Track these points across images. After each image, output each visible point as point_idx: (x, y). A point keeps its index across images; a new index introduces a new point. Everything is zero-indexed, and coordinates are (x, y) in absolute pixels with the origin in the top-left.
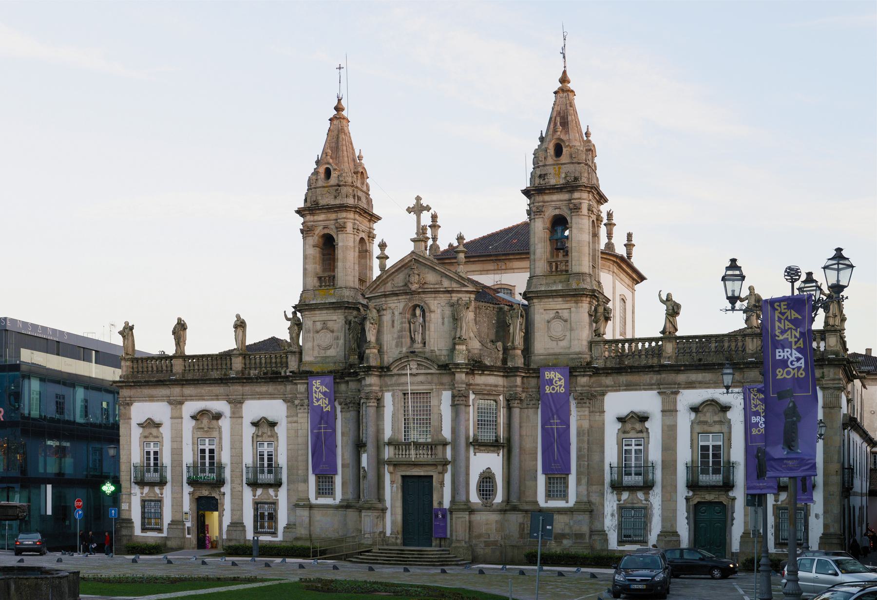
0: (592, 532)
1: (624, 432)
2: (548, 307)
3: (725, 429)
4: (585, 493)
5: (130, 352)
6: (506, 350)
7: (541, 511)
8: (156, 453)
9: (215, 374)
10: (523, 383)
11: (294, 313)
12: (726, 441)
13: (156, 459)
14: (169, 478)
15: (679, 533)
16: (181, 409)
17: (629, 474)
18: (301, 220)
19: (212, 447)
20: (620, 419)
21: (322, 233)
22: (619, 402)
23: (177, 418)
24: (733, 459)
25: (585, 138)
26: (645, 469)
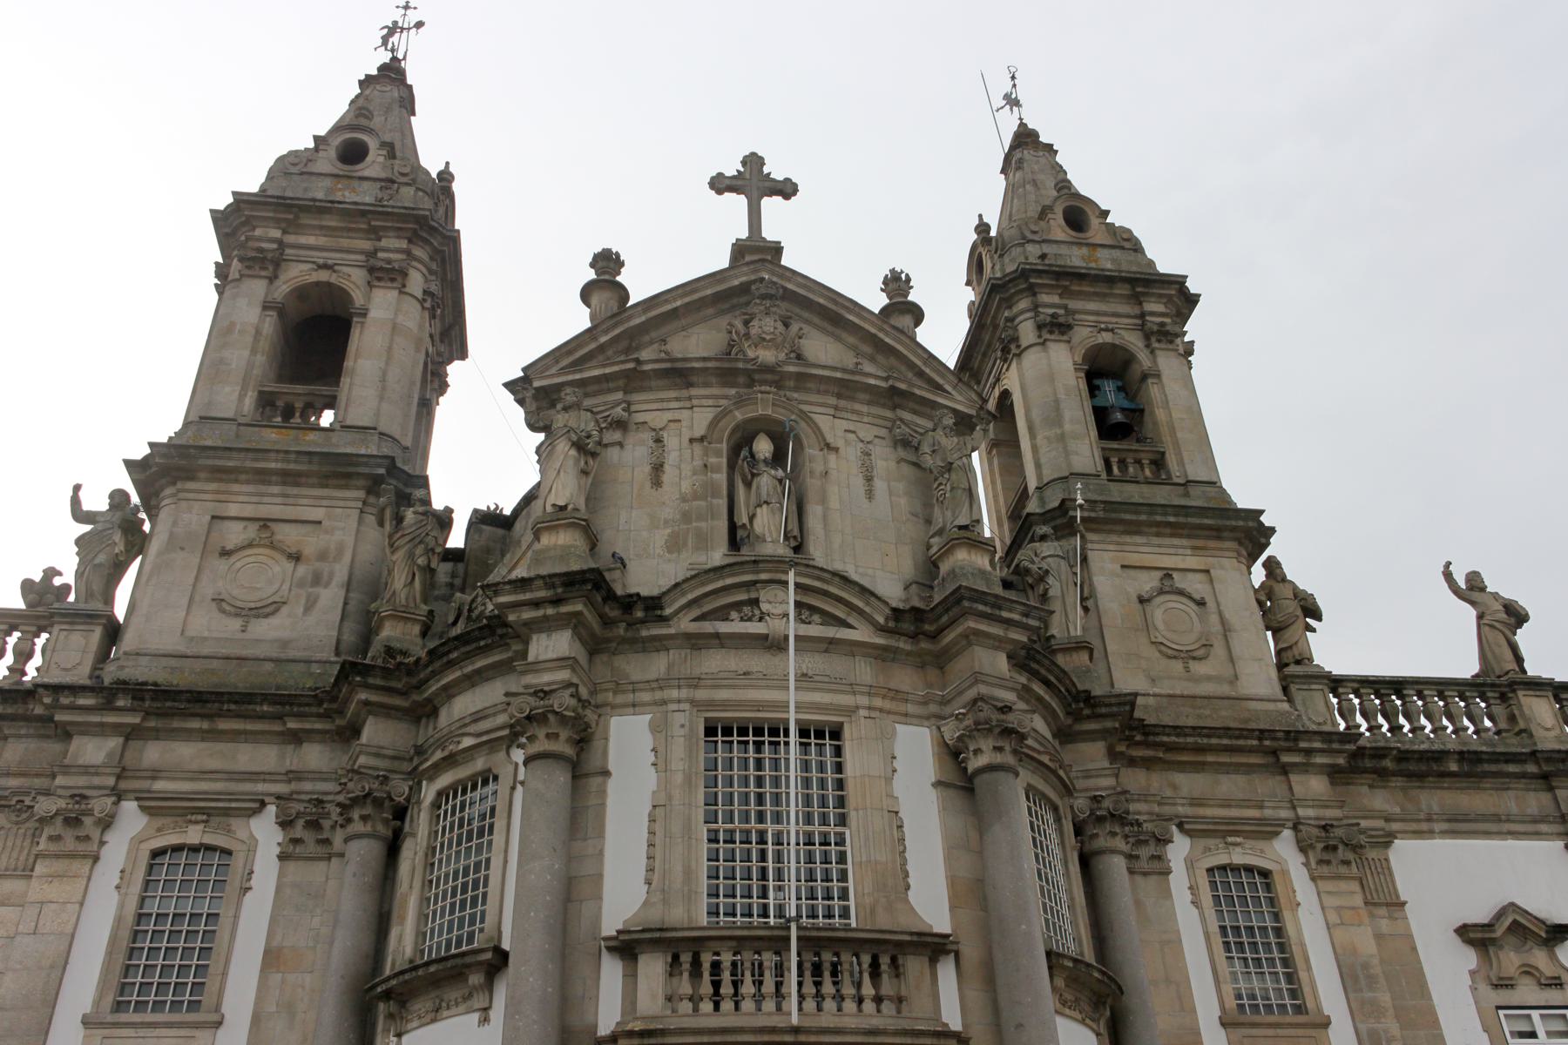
1: (1503, 984)
2: (1134, 559)
11: (118, 498)
20: (1469, 934)
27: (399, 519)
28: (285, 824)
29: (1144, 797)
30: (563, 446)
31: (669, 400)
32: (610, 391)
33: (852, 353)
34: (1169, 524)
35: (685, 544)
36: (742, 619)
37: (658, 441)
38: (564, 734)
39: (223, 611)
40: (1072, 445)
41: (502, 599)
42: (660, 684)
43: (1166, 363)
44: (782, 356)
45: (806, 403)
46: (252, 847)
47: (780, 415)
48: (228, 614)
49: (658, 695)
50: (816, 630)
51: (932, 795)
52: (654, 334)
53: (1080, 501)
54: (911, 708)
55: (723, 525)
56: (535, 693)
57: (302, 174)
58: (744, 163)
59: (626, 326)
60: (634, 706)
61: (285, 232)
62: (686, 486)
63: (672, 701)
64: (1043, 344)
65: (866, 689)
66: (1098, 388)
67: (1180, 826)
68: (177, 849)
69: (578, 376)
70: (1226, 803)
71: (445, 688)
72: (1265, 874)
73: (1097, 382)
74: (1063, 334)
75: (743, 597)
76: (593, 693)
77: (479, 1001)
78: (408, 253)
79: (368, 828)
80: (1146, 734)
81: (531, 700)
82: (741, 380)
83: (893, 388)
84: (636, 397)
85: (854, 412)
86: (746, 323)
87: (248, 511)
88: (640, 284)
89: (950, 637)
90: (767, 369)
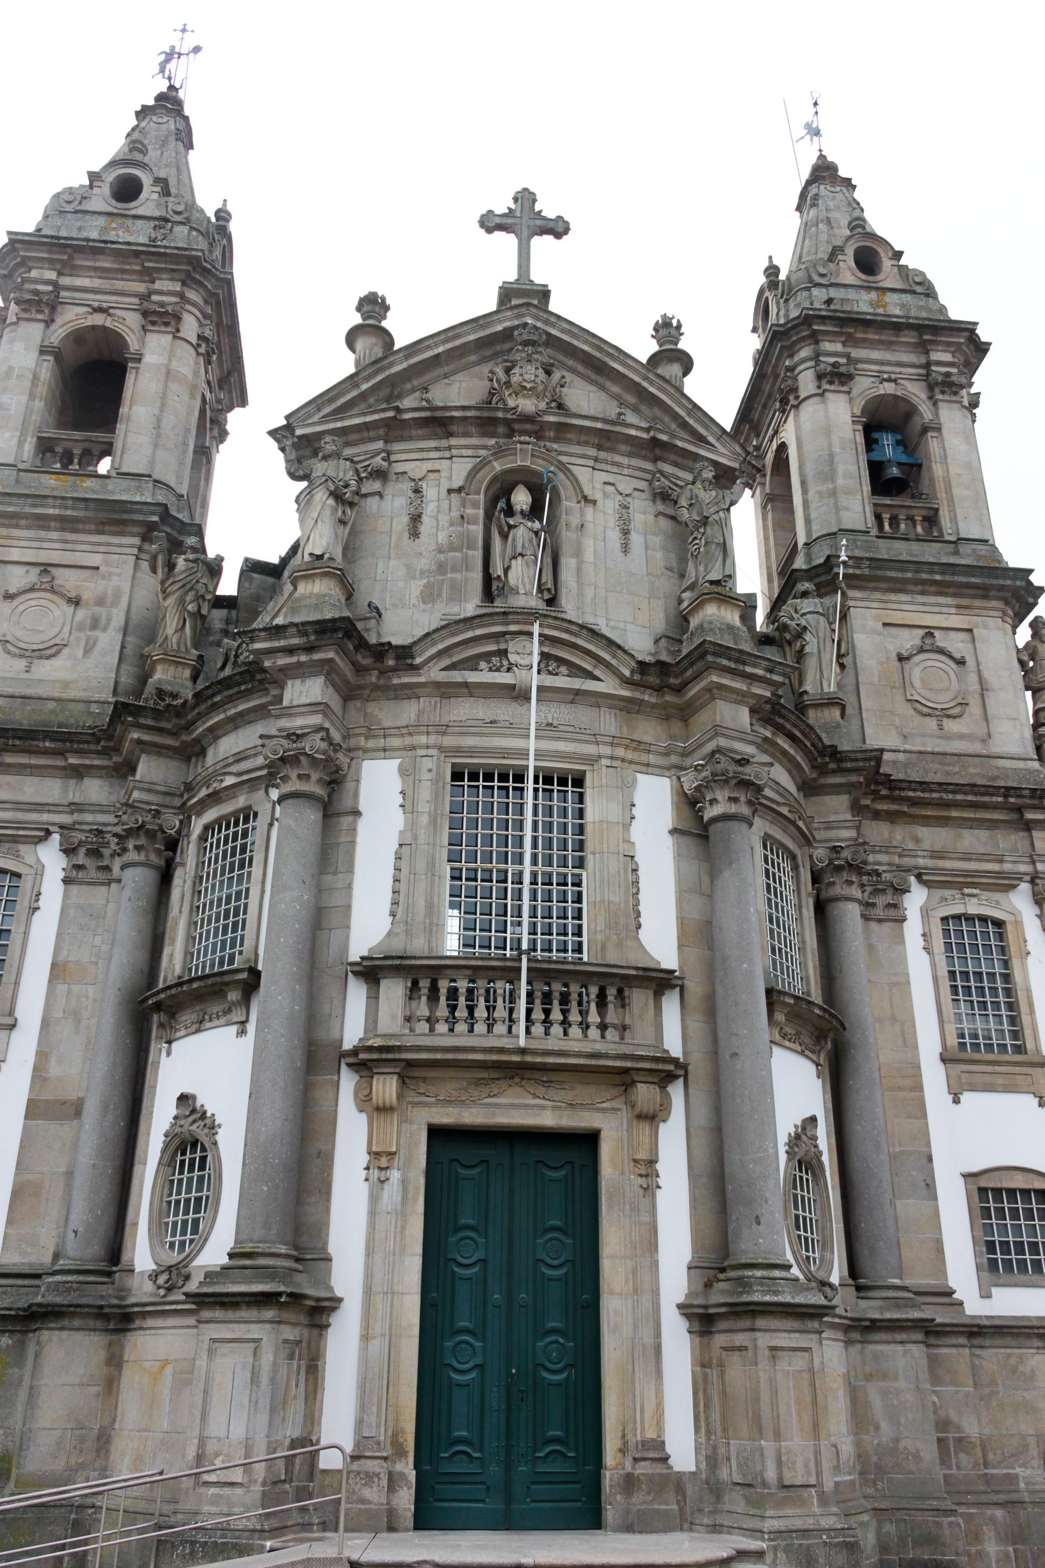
7: (981, 1332)
27: (171, 566)
28: (68, 851)
29: (886, 849)
30: (321, 495)
31: (429, 450)
32: (371, 440)
33: (616, 403)
34: (934, 582)
35: (439, 595)
36: (491, 670)
37: (417, 491)
38: (315, 776)
39: (9, 652)
40: (843, 501)
41: (257, 646)
42: (410, 730)
43: (949, 416)
44: (542, 405)
45: (566, 454)
46: (39, 871)
47: (538, 466)
48: (14, 655)
49: (408, 741)
50: (562, 681)
52: (416, 383)
53: (844, 558)
54: (652, 759)
55: (476, 577)
56: (288, 737)
57: (76, 212)
58: (516, 200)
59: (387, 373)
60: (385, 750)
61: (60, 274)
62: (442, 537)
63: (421, 747)
64: (822, 395)
65: (610, 740)
66: (876, 441)
67: (919, 877)
69: (339, 425)
70: (966, 857)
71: (211, 729)
72: (999, 924)
73: (875, 435)
74: (843, 384)
75: (493, 647)
76: (346, 737)
77: (238, 1015)
78: (181, 295)
79: (142, 857)
80: (890, 789)
81: (284, 742)
82: (501, 430)
83: (654, 438)
84: (397, 446)
85: (614, 464)
86: (508, 371)
87: (30, 556)
88: (405, 328)
89: (693, 690)
90: (527, 418)
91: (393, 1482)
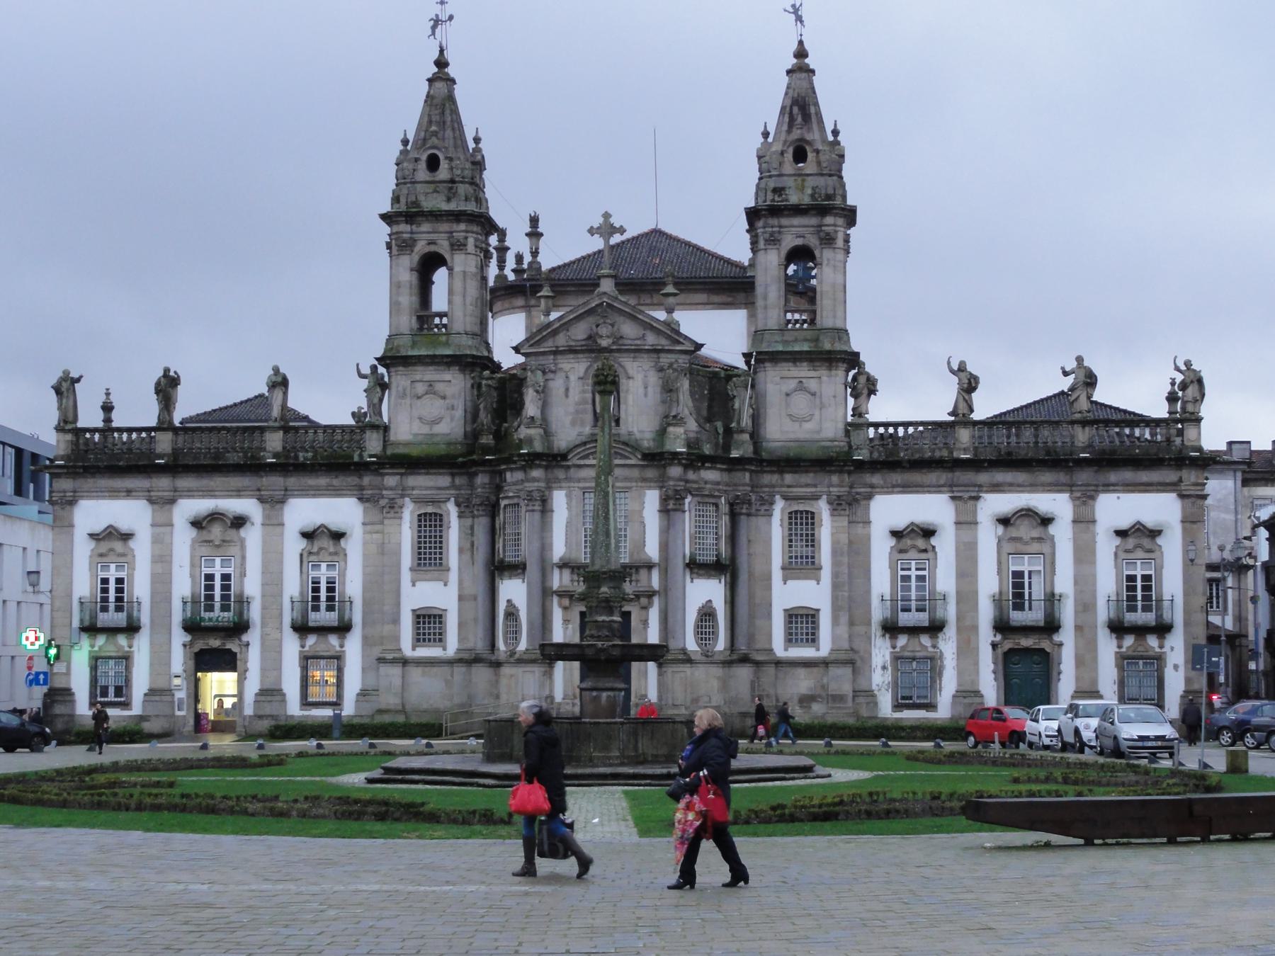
0: (856, 693)
1: (901, 551)
2: (786, 373)
3: (1046, 548)
4: (846, 636)
5: (71, 419)
6: (728, 432)
7: (779, 663)
8: (120, 581)
9: (233, 458)
10: (751, 479)
11: (374, 368)
12: (1048, 566)
13: (119, 590)
14: (145, 619)
15: (983, 692)
16: (170, 511)
17: (907, 609)
18: (387, 230)
19: (226, 571)
21: (427, 249)
22: (891, 509)
23: (162, 525)
24: (1057, 591)
25: (831, 138)
26: (929, 601)
28: (458, 504)
51: (657, 515)
68: (425, 514)
72: (813, 513)
91: (574, 705)
